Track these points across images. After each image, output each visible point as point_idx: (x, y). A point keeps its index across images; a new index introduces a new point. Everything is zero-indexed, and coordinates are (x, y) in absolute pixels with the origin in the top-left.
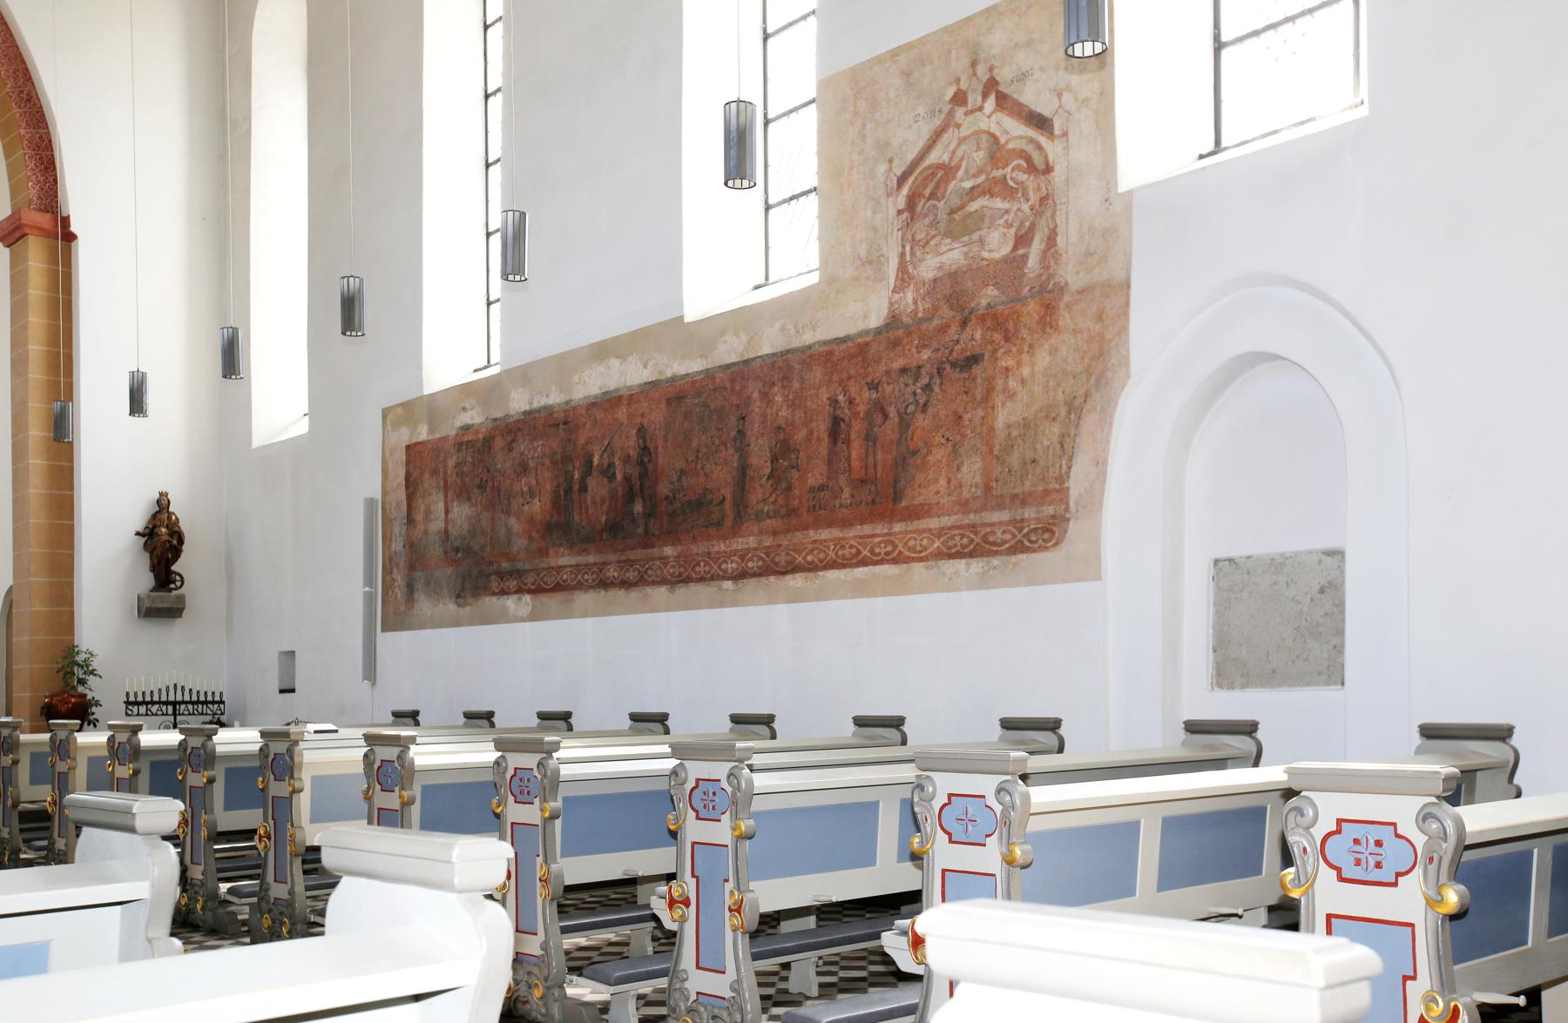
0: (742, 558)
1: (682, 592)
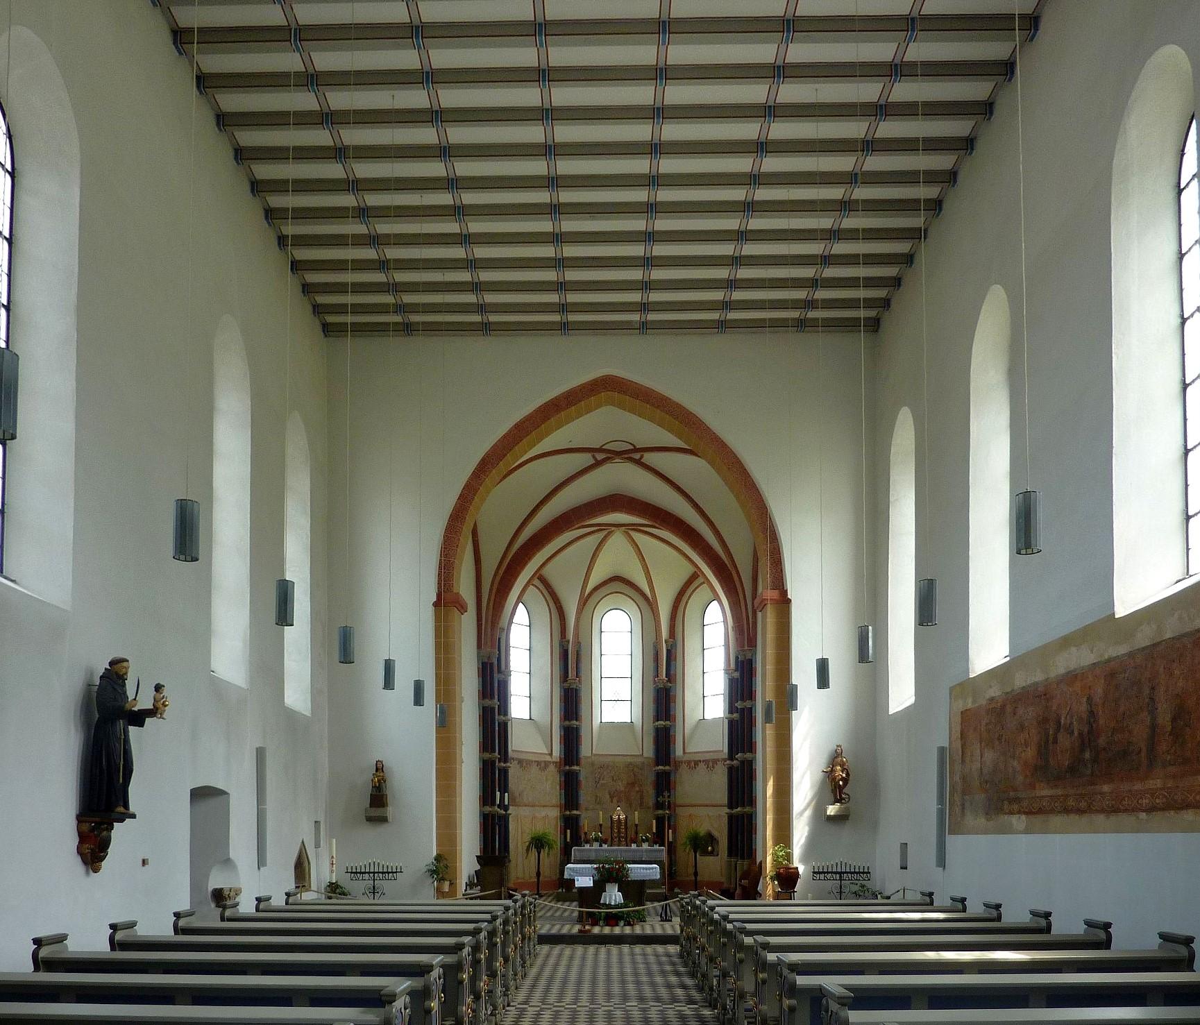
0: (1152, 795)
1: (1113, 818)
